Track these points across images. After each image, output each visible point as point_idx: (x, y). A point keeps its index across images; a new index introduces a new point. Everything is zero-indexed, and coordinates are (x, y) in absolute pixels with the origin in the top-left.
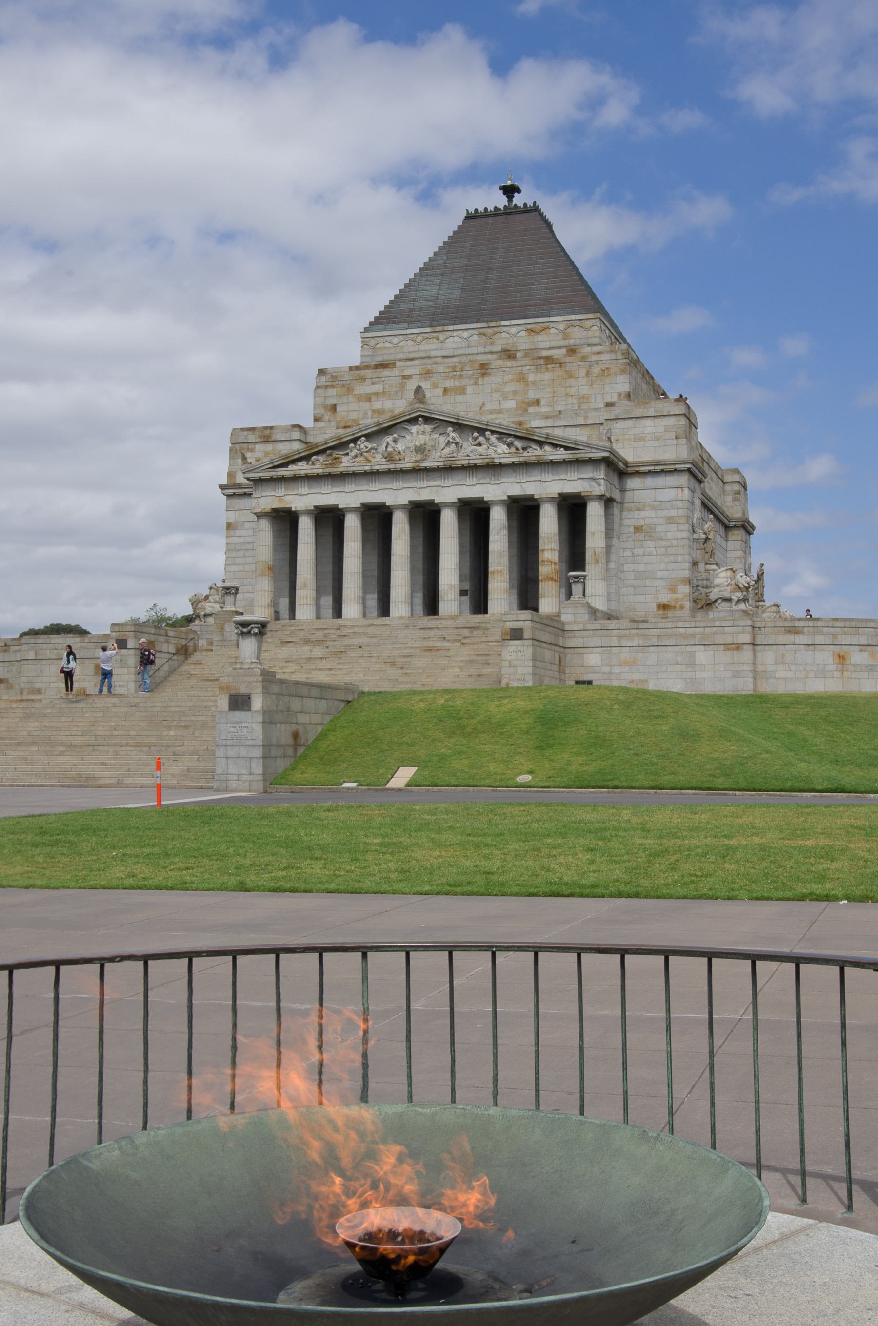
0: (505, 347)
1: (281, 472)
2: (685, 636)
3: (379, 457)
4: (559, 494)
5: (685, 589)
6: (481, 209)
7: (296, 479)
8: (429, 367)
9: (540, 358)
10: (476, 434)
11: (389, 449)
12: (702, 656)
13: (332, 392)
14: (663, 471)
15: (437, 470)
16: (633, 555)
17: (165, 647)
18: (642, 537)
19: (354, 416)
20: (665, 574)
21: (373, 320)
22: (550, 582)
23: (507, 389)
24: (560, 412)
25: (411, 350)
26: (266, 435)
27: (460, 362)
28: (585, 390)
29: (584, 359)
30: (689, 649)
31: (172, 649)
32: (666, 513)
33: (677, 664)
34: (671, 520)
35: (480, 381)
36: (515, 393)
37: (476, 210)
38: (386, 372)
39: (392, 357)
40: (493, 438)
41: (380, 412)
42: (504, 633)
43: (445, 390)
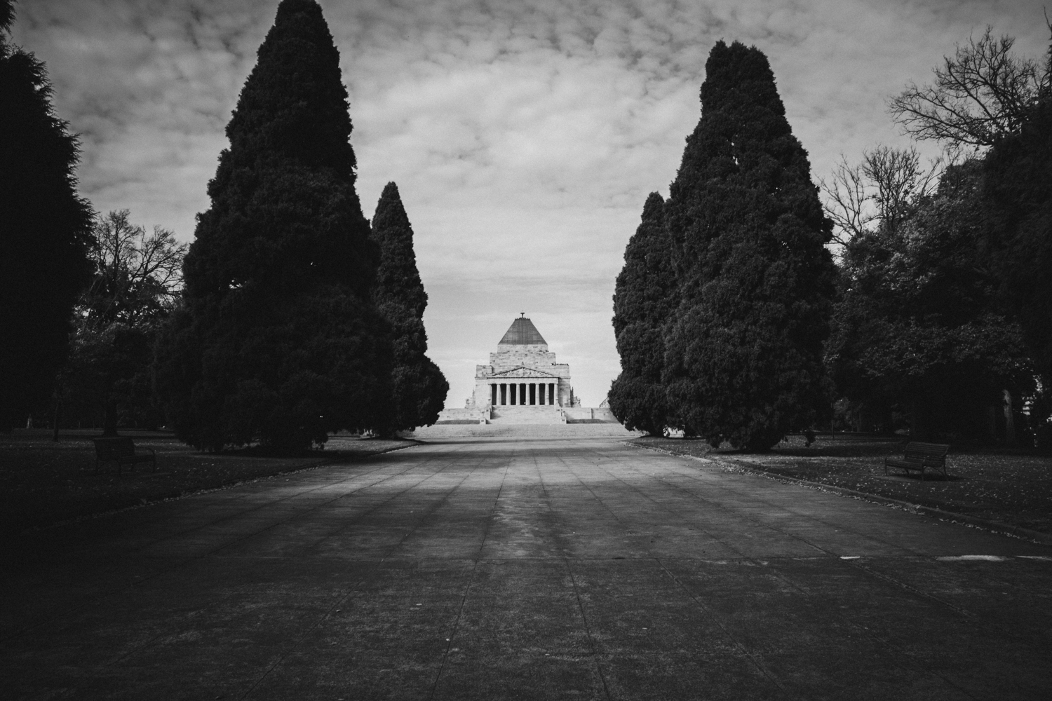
12: (583, 414)
26: (484, 367)
41: (504, 363)
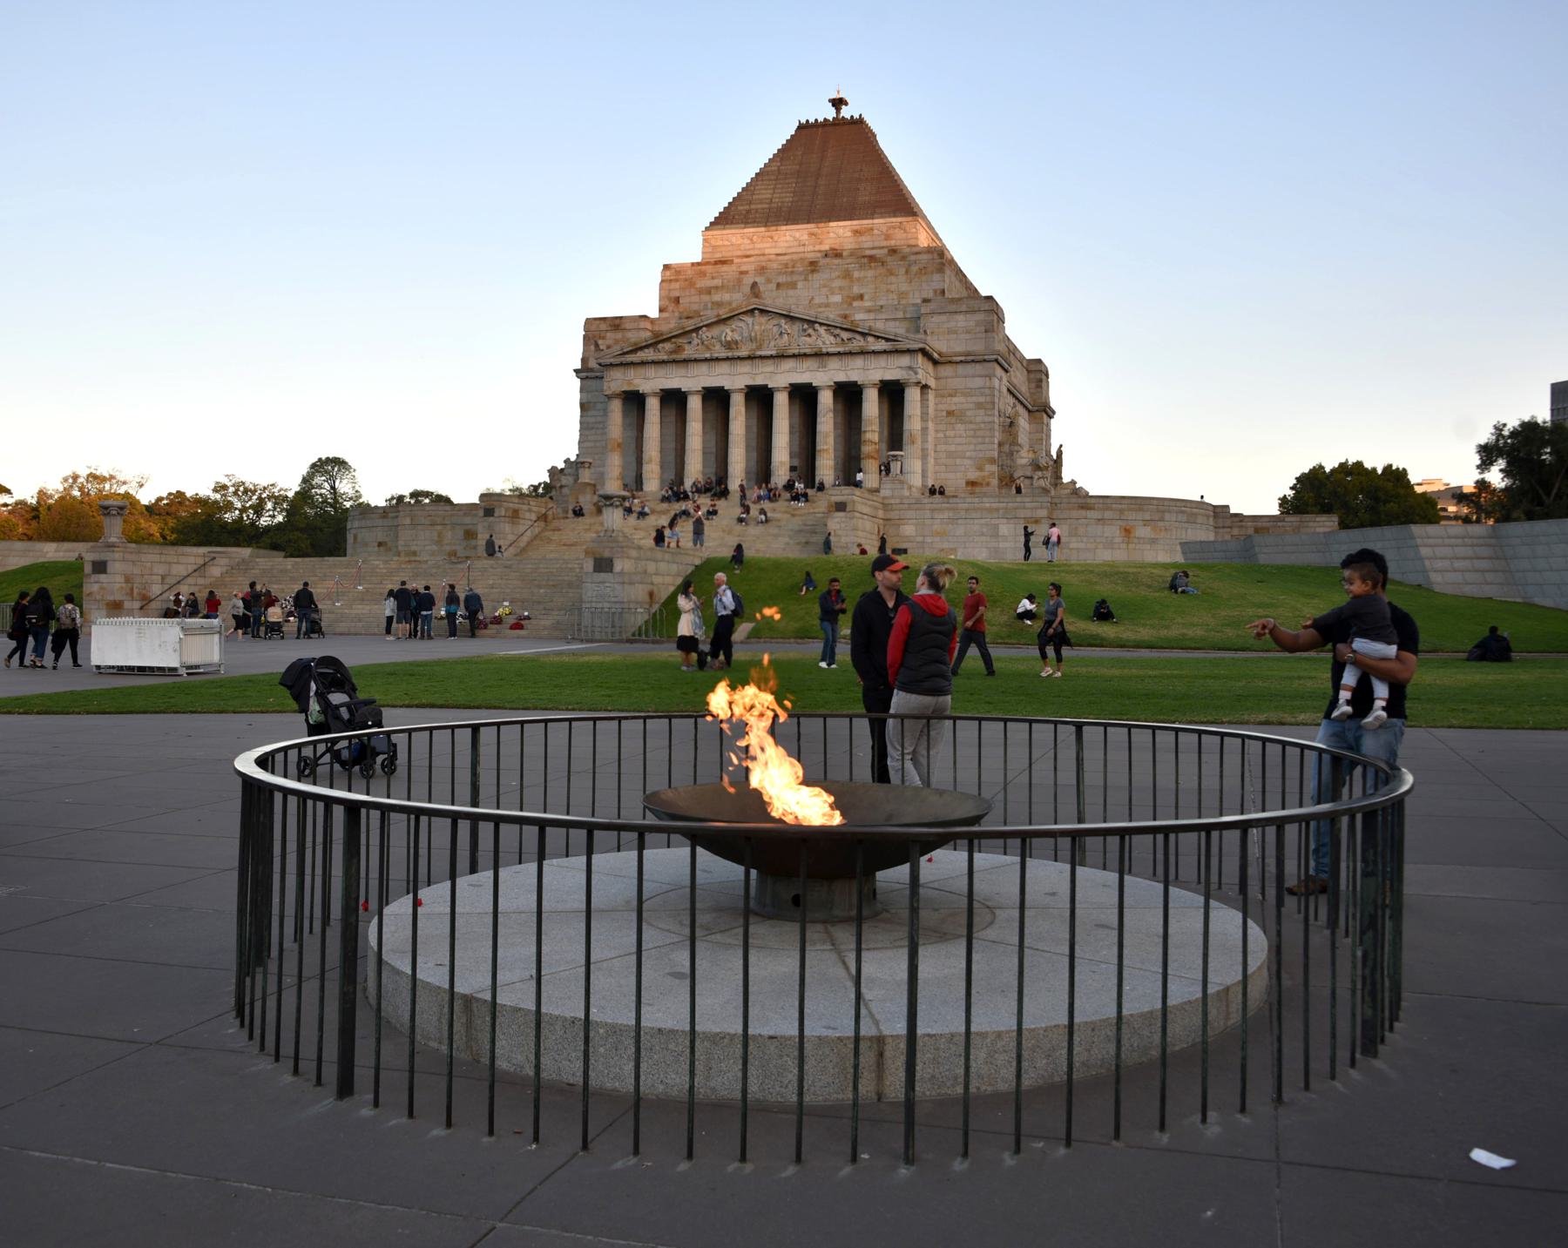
0: (833, 246)
1: (630, 358)
2: (990, 510)
3: (718, 347)
4: (881, 381)
5: (994, 468)
6: (812, 120)
7: (643, 363)
8: (764, 264)
9: (864, 257)
10: (806, 326)
11: (729, 339)
13: (676, 285)
14: (973, 361)
15: (771, 357)
16: (945, 437)
17: (527, 515)
18: (953, 421)
19: (695, 307)
20: (974, 454)
21: (713, 220)
22: (874, 461)
23: (834, 285)
24: (882, 307)
25: (748, 247)
27: (792, 260)
28: (904, 287)
29: (903, 258)
30: (993, 521)
31: (534, 517)
32: (974, 399)
33: (983, 534)
34: (979, 406)
35: (810, 277)
36: (841, 288)
37: (807, 121)
38: (725, 268)
39: (730, 254)
40: (822, 330)
41: (719, 304)
42: (830, 506)
43: (778, 285)
